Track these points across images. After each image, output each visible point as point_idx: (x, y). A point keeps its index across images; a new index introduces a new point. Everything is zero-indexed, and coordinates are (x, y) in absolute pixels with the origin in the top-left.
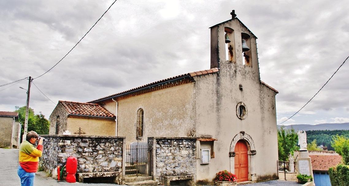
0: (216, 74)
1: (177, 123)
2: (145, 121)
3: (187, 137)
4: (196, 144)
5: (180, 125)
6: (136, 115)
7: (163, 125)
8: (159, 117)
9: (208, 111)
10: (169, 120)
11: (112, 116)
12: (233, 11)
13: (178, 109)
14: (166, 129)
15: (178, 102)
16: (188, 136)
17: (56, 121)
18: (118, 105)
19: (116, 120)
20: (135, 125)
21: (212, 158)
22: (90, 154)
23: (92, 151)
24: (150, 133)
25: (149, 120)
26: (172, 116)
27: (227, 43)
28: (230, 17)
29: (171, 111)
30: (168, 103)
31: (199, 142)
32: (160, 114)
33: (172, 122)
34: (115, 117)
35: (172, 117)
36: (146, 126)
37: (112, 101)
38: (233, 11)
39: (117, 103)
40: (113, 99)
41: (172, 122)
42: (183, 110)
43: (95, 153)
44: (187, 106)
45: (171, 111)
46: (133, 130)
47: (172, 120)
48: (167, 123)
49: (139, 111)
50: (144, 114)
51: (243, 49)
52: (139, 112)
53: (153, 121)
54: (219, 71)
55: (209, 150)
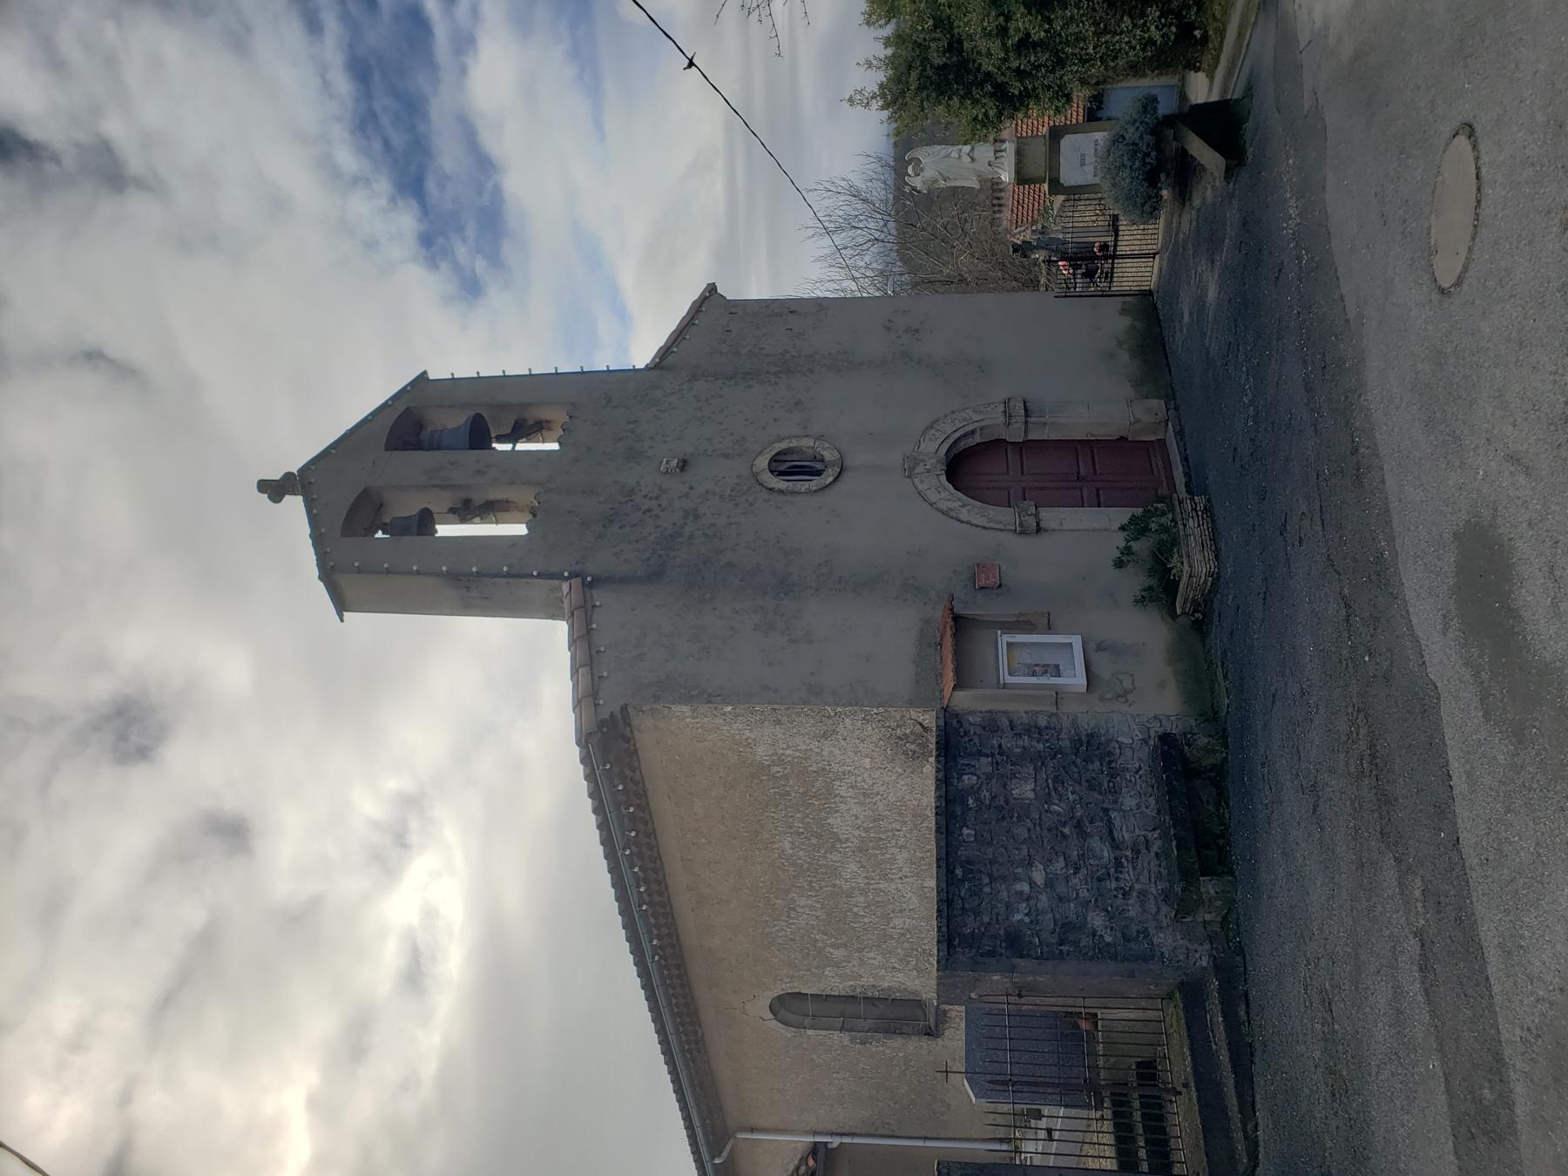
0: (595, 593)
1: (856, 810)
3: (932, 759)
4: (972, 713)
6: (809, 1032)
7: (864, 892)
8: (819, 914)
11: (811, 1162)
14: (885, 876)
16: (925, 756)
18: (752, 1130)
19: (835, 1142)
20: (863, 1043)
26: (815, 841)
27: (437, 527)
28: (294, 505)
31: (958, 694)
32: (803, 901)
33: (847, 840)
34: (815, 1149)
35: (819, 836)
36: (867, 981)
37: (731, 1161)
38: (266, 487)
39: (740, 1136)
41: (847, 840)
42: (786, 777)
45: (787, 845)
48: (853, 867)
50: (803, 991)
51: (472, 448)
54: (578, 576)
55: (1007, 638)
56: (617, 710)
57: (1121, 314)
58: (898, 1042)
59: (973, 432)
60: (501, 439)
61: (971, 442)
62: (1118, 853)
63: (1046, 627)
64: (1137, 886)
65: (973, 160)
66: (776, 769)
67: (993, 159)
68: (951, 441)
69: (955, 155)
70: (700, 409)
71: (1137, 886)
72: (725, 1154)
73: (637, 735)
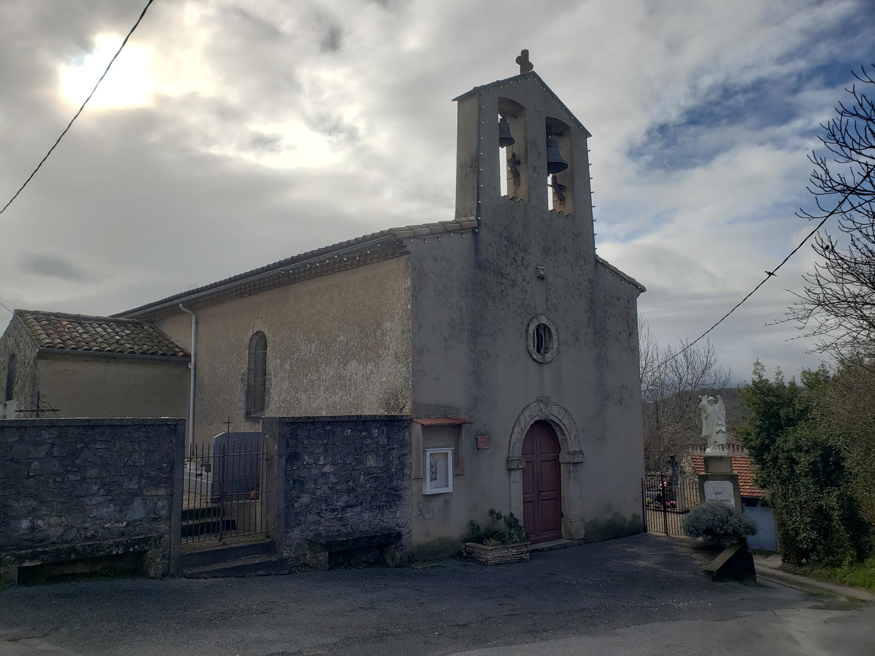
0: (470, 234)
1: (360, 374)
2: (271, 368)
3: (386, 413)
4: (410, 434)
5: (367, 378)
6: (247, 352)
7: (319, 378)
8: (307, 355)
9: (446, 339)
10: (336, 365)
11: (181, 354)
12: (525, 53)
13: (360, 332)
14: (327, 389)
15: (362, 313)
16: (387, 410)
17: (7, 371)
18: (197, 323)
19: (192, 366)
20: (242, 380)
21: (456, 475)
22: (55, 481)
23: (61, 470)
24: (283, 402)
25: (282, 366)
26: (344, 352)
27: (505, 148)
28: (515, 70)
29: (341, 338)
30: (334, 317)
31: (420, 427)
32: (313, 347)
33: (345, 369)
34: (187, 356)
35: (346, 355)
36: (274, 381)
37: (181, 312)
38: (525, 53)
39: (194, 317)
40: (180, 305)
41: (345, 369)
42: (376, 337)
43: (72, 477)
44: (388, 325)
45: (341, 338)
46: (238, 393)
47: (345, 365)
48: (331, 373)
49: (256, 338)
50: (268, 349)
51: (548, 163)
52: (254, 343)
53: (291, 367)
54: (479, 224)
55: (450, 452)
56: (408, 249)
57: (633, 515)
58: (243, 398)
59: (564, 434)
60: (554, 179)
61: (558, 433)
62: (340, 510)
63: (457, 474)
64: (323, 520)
65: (717, 433)
66: (379, 332)
67: (718, 444)
68: (558, 422)
69: (720, 422)
70: (573, 285)
71: (323, 520)
72: (184, 309)
73: (396, 259)
